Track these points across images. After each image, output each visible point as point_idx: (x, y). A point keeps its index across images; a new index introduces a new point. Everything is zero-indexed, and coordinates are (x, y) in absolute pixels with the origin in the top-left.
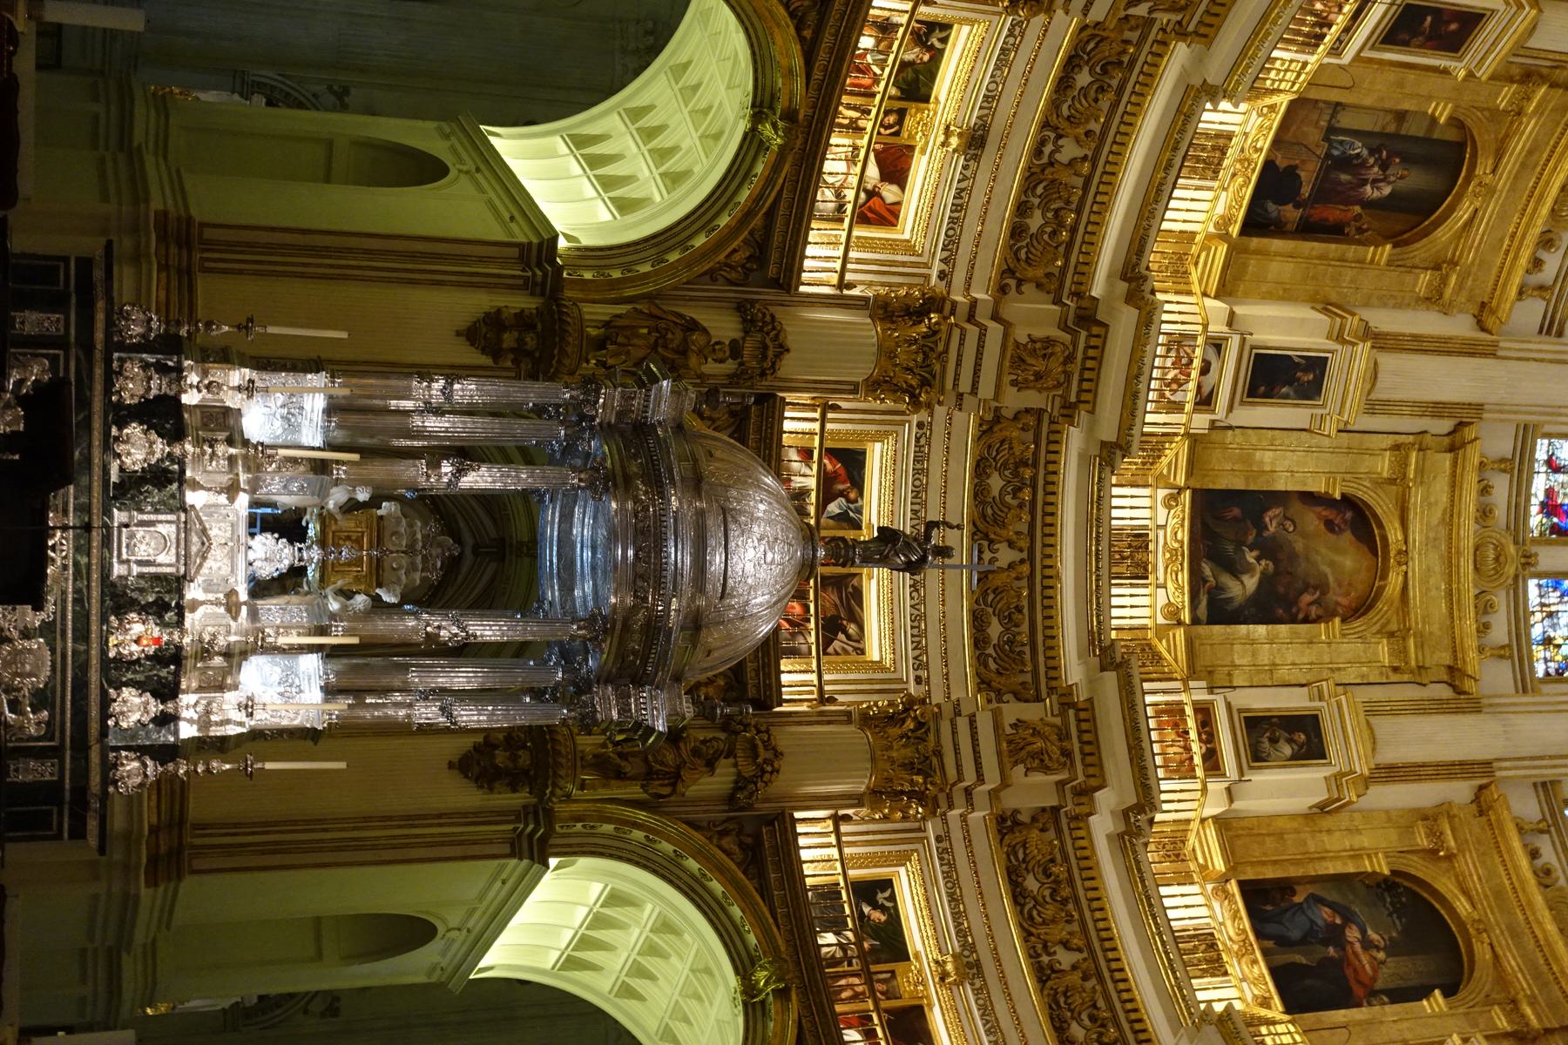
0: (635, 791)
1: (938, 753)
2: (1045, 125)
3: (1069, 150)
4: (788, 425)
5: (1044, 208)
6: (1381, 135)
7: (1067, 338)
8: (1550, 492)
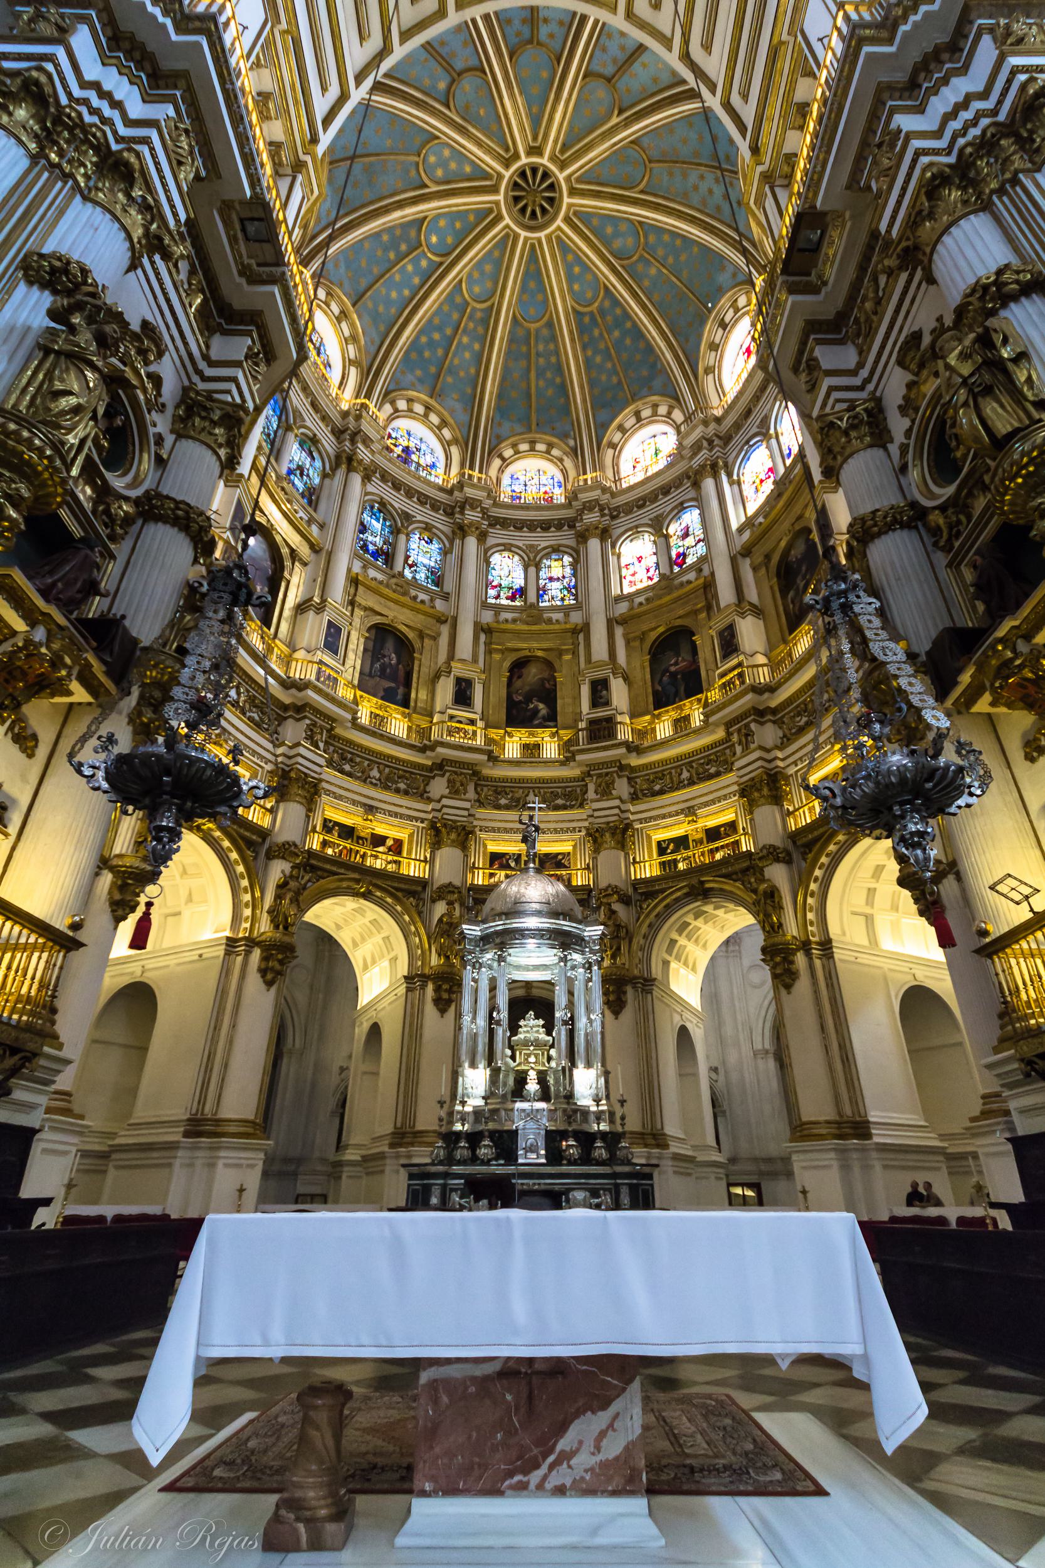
1: (608, 823)
2: (365, 781)
3: (375, 773)
4: (480, 883)
5: (397, 782)
6: (372, 657)
7: (448, 774)
8: (507, 598)
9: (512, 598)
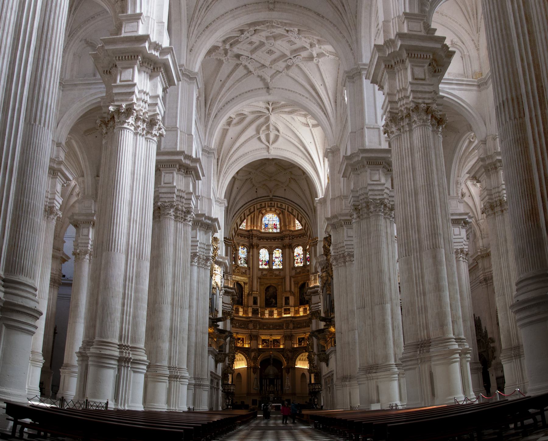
0: (290, 361)
3: (237, 325)
9: (266, 265)
